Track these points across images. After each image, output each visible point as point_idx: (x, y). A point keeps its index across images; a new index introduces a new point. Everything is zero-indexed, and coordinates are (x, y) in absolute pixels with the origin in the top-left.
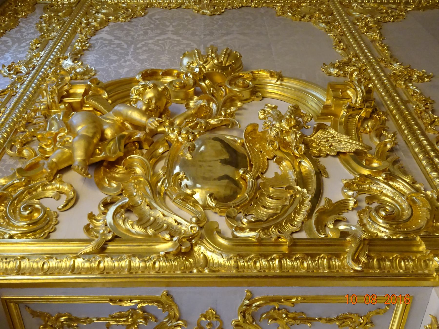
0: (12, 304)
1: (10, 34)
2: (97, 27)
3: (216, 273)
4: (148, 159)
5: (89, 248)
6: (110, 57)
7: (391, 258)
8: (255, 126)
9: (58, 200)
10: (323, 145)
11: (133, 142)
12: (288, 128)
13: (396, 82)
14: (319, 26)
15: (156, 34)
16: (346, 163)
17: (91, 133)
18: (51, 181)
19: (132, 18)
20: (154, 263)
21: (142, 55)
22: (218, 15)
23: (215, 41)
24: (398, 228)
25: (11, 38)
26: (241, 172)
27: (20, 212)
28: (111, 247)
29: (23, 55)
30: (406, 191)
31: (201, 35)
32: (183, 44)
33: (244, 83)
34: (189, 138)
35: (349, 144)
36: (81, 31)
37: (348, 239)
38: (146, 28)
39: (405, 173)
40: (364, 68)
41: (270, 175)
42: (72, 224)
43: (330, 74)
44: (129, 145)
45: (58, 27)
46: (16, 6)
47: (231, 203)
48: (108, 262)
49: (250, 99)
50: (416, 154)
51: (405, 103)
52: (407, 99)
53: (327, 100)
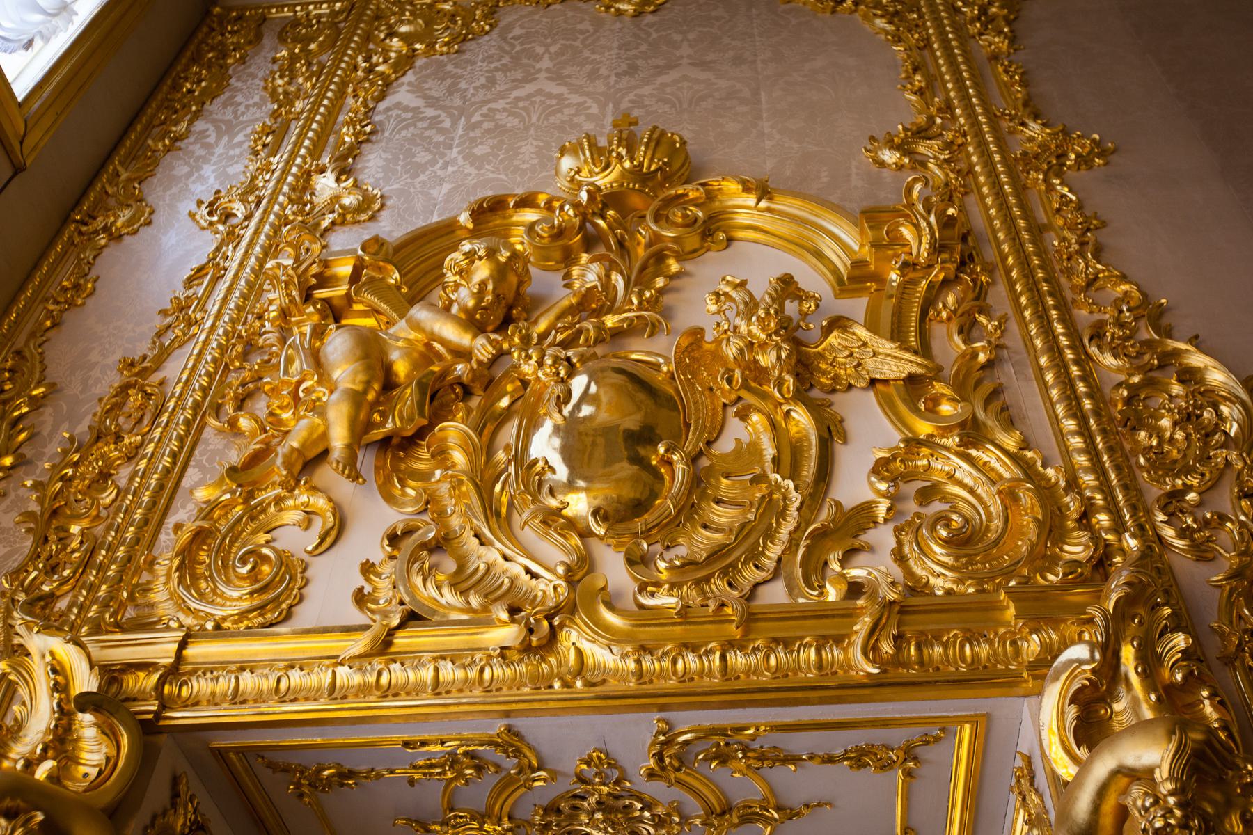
0: (232, 755)
1: (211, 113)
2: (389, 76)
3: (598, 689)
4: (475, 430)
5: (359, 644)
6: (414, 156)
7: (945, 639)
8: (697, 333)
9: (307, 529)
10: (842, 364)
11: (451, 385)
12: (763, 336)
13: (1028, 173)
14: (874, 24)
15: (513, 81)
16: (887, 404)
17: (361, 382)
18: (291, 491)
19: (464, 40)
20: (482, 670)
21: (481, 143)
22: (652, 12)
23: (638, 91)
24: (972, 565)
25: (214, 122)
26: (662, 450)
27: (234, 566)
28: (402, 641)
29: (239, 168)
30: (1001, 470)
31: (609, 76)
32: (569, 105)
33: (685, 216)
34: (558, 374)
35: (893, 362)
36: (354, 91)
37: (860, 602)
38: (492, 66)
39: (1009, 423)
40: (960, 141)
41: (725, 445)
42: (331, 588)
43: (882, 164)
44: (440, 395)
45: (309, 84)
46: (223, 35)
47: (639, 524)
48: (397, 674)
49: (702, 247)
50: (1040, 370)
51: (1038, 231)
52: (1045, 221)
53: (862, 246)
